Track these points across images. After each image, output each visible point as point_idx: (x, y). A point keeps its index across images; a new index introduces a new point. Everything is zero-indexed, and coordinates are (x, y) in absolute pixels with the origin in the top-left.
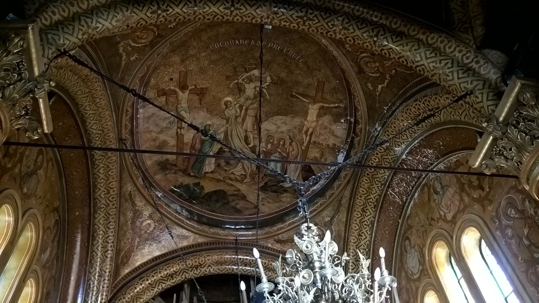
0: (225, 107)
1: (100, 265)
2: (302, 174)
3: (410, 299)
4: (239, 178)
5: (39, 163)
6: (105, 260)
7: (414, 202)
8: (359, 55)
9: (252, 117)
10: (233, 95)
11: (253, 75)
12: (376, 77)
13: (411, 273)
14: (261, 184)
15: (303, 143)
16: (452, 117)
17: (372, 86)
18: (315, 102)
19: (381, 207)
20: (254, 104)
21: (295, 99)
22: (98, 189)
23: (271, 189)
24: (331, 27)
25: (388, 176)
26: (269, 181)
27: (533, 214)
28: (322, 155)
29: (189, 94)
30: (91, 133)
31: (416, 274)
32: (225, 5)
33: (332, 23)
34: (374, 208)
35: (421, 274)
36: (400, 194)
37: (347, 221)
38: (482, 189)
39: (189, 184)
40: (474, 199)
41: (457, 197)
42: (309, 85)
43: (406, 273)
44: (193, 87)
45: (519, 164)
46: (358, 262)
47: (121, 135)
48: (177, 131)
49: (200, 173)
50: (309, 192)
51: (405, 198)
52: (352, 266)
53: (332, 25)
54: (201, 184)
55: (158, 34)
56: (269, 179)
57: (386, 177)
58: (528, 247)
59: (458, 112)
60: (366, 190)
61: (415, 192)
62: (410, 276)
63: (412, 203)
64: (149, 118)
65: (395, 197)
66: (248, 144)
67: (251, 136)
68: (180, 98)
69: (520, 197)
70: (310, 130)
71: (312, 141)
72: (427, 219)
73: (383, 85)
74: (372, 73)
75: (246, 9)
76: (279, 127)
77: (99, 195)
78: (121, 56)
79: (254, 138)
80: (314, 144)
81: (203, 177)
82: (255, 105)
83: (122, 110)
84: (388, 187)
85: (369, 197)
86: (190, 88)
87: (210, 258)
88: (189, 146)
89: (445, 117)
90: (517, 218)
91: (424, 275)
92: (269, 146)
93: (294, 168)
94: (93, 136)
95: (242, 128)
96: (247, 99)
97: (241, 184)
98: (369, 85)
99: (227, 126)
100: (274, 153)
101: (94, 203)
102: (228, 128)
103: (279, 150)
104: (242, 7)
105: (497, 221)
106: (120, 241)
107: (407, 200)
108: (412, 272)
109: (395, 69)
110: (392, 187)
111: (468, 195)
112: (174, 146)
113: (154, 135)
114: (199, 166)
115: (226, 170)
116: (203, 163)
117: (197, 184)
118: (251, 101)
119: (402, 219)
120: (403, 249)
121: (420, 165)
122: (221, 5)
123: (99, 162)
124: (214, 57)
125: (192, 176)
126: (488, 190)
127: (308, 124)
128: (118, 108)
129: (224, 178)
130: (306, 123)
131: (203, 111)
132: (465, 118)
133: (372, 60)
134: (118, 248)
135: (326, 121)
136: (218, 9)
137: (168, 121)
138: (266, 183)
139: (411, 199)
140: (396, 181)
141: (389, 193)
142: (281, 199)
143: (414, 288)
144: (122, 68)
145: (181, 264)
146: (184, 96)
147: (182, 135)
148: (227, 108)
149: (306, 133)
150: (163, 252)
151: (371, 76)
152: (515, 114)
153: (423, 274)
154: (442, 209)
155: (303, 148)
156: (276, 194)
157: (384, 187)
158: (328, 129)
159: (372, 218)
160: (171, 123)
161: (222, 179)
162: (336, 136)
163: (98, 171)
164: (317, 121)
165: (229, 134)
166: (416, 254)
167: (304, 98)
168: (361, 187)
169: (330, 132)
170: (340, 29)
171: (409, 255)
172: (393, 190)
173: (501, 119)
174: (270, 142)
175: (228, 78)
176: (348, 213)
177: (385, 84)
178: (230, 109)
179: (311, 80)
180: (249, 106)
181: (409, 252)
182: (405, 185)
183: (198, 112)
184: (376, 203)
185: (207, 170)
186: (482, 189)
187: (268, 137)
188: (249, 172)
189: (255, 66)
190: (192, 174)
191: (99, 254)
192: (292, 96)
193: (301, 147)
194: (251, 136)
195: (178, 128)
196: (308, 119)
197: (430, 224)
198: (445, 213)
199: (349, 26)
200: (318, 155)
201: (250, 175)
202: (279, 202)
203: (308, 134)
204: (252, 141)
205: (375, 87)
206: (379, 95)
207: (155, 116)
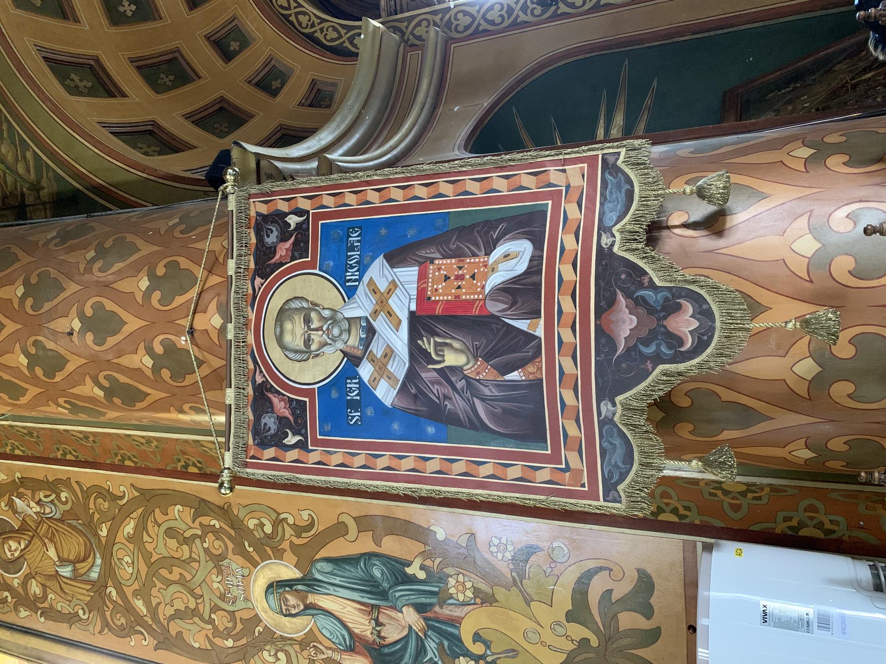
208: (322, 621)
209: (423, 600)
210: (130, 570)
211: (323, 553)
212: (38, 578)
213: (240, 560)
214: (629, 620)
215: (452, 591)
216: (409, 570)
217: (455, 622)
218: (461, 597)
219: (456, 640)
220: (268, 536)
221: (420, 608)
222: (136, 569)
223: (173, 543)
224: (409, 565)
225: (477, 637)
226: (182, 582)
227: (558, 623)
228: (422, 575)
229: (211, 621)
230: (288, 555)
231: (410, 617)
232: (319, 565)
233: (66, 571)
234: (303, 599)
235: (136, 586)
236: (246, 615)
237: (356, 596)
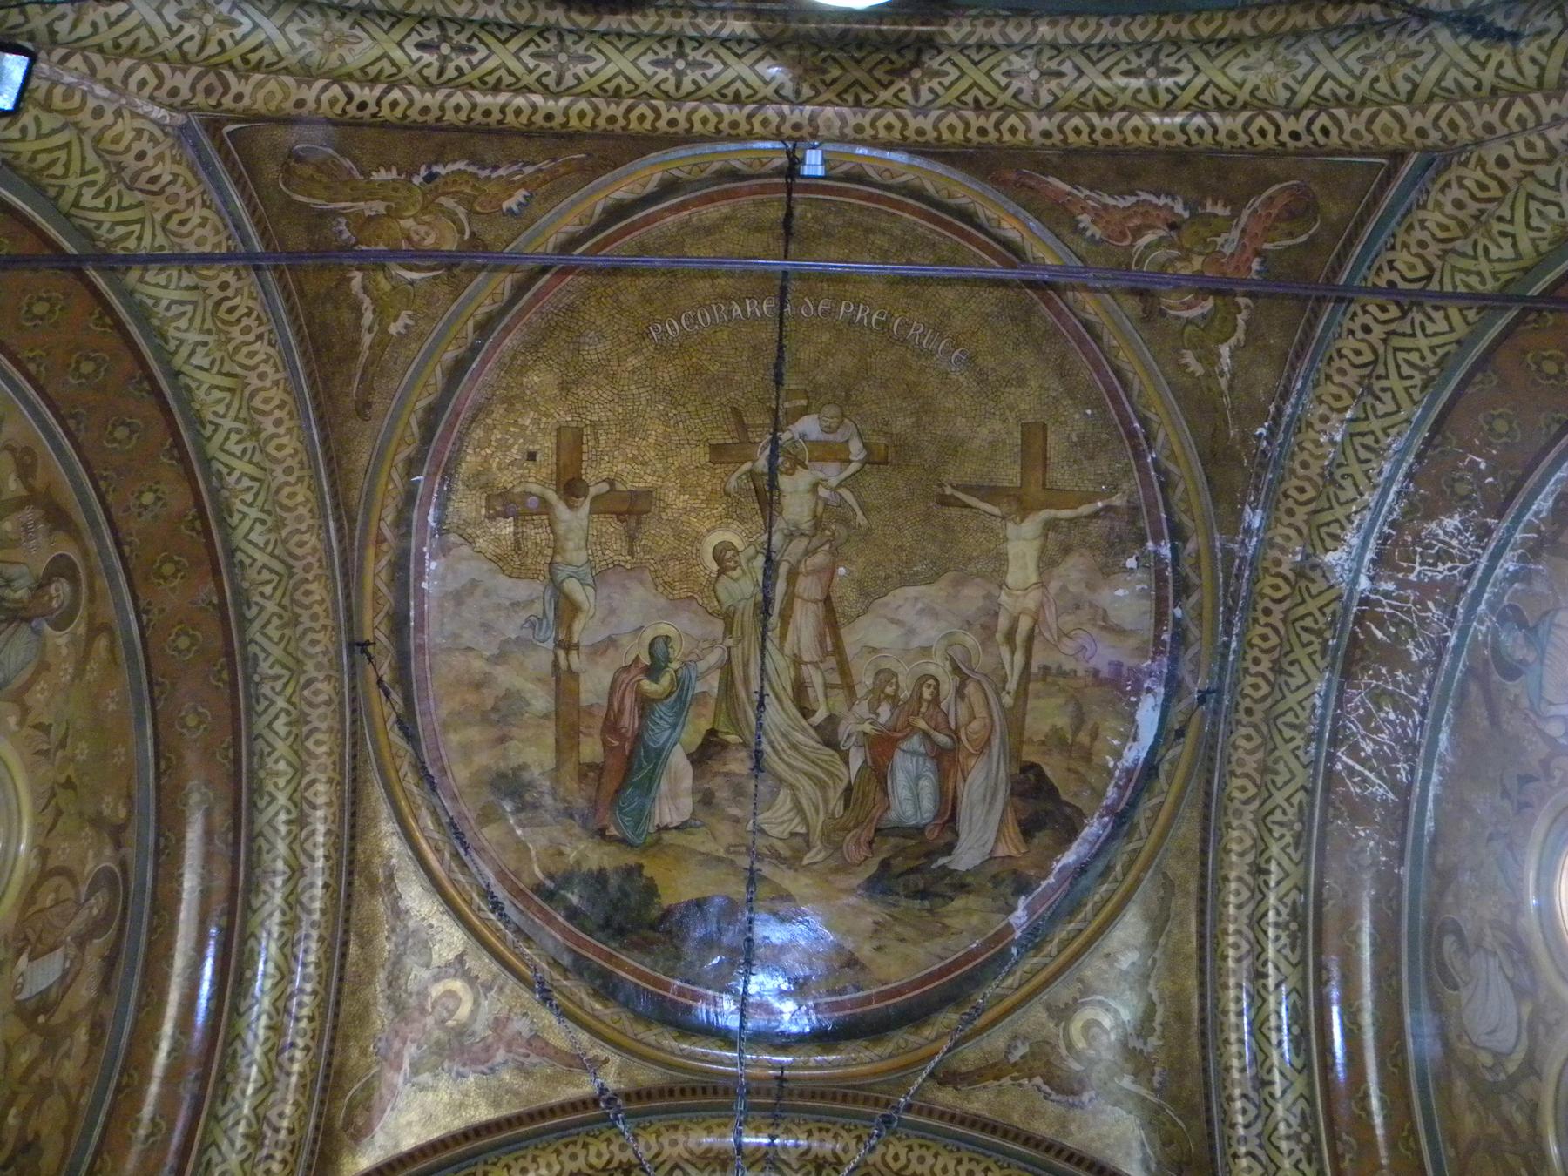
0: (715, 567)
1: (257, 1091)
2: (1016, 811)
4: (785, 852)
5: (55, 604)
6: (275, 1080)
7: (1441, 773)
8: (1132, 245)
9: (812, 607)
10: (742, 520)
11: (803, 436)
12: (1204, 316)
14: (873, 867)
15: (1004, 680)
17: (1199, 360)
18: (1024, 509)
20: (815, 552)
21: (954, 512)
22: (267, 798)
23: (906, 886)
24: (1003, 81)
25: (1326, 698)
26: (899, 851)
28: (1079, 719)
29: (591, 512)
30: (248, 561)
32: (656, 53)
33: (1004, 66)
34: (1296, 848)
36: (1384, 761)
37: (1201, 947)
39: (602, 871)
42: (993, 445)
44: (605, 487)
46: (1268, 1089)
47: (361, 630)
48: (556, 656)
49: (639, 830)
50: (1051, 880)
51: (1403, 776)
52: (1244, 1112)
53: (1007, 74)
54: (647, 872)
55: (473, 234)
56: (896, 846)
57: (1318, 702)
60: (1254, 783)
61: (1436, 729)
63: (1435, 778)
64: (459, 597)
65: (1365, 780)
66: (806, 713)
67: (817, 680)
68: (561, 529)
70: (1024, 624)
71: (1034, 669)
73: (1232, 341)
74: (1190, 307)
75: (724, 63)
76: (911, 632)
77: (270, 823)
78: (357, 309)
79: (827, 686)
80: (1044, 680)
81: (652, 846)
82: (820, 559)
83: (366, 524)
84: (1335, 742)
85: (1269, 806)
86: (593, 491)
87: (680, 1136)
88: (598, 723)
92: (885, 712)
93: (981, 790)
94: (252, 573)
95: (781, 650)
96: (790, 536)
97: (791, 873)
98: (1189, 357)
99: (730, 642)
100: (905, 738)
101: (250, 851)
102: (734, 651)
103: (922, 724)
104: (711, 59)
106: (346, 1038)
107: (1412, 771)
109: (1258, 253)
110: (1346, 738)
112: (546, 716)
113: (478, 665)
114: (637, 801)
115: (736, 820)
116: (650, 789)
117: (632, 872)
118: (805, 541)
119: (1408, 862)
120: (1434, 971)
121: (1430, 604)
122: (645, 53)
123: (273, 689)
124: (668, 373)
125: (612, 840)
127: (1010, 601)
128: (352, 520)
129: (727, 851)
130: (1004, 598)
131: (642, 582)
133: (1176, 253)
134: (336, 1061)
135: (1074, 575)
136: (634, 62)
137: (524, 615)
138: (885, 865)
139: (1428, 764)
140: (1356, 708)
141: (1339, 767)
142: (947, 921)
144: (362, 360)
145: (566, 1153)
146: (574, 520)
147: (573, 675)
148: (722, 571)
149: (1010, 636)
150: (504, 1112)
151: (1189, 321)
155: (1008, 700)
156: (927, 904)
157: (1318, 748)
158: (1086, 606)
159: (1294, 894)
160: (533, 626)
161: (721, 853)
162: (1118, 631)
163: (269, 725)
164: (1042, 584)
165: (738, 672)
167: (982, 499)
168: (1233, 773)
169: (1093, 620)
170: (1034, 82)
172: (1354, 751)
174: (888, 696)
175: (719, 453)
176: (1201, 913)
177: (1240, 334)
178: (735, 574)
179: (998, 426)
180: (799, 562)
182: (1392, 716)
183: (624, 586)
184: (1297, 826)
185: (667, 820)
187: (877, 674)
188: (818, 821)
189: (804, 402)
190: (613, 831)
191: (258, 1053)
192: (945, 501)
193: (999, 699)
194: (817, 680)
195: (559, 644)
196: (1010, 580)
199: (1060, 64)
200: (1063, 721)
201: (826, 837)
202: (940, 935)
203: (1020, 638)
204: (821, 698)
205: (1210, 358)
206: (1231, 388)
207: (479, 592)
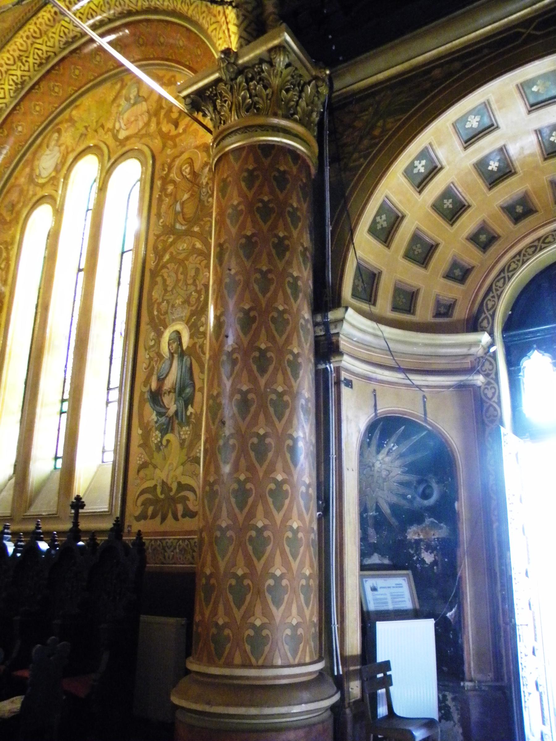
3: (18, 202)
13: (37, 174)
16: (201, 18)
19: (48, 72)
27: (204, 184)
31: (42, 178)
35: (48, 182)
38: (176, 125)
40: (160, 132)
41: (145, 118)
43: (32, 170)
45: (222, 122)
58: (176, 213)
59: (211, 19)
62: (34, 176)
69: (206, 159)
72: (97, 122)
89: (194, 12)
90: (187, 178)
91: (53, 184)
105: (166, 169)
108: (40, 174)
111: (158, 123)
126: (181, 131)
132: (212, 31)
143: (31, 193)
152: (257, 66)
153: (52, 182)
154: (121, 121)
166: (58, 155)
171: (48, 152)
173: (240, 62)
181: (51, 147)
186: (176, 125)
197: (96, 131)
198: (120, 128)
208: (168, 363)
209: (179, 414)
210: (181, 248)
211: (194, 361)
212: (174, 190)
213: (188, 314)
214: (180, 507)
215: (184, 429)
216: (190, 407)
217: (172, 430)
218: (182, 433)
219: (166, 433)
220: (198, 329)
221: (176, 413)
222: (181, 252)
223: (192, 273)
224: (192, 407)
225: (168, 441)
226: (178, 281)
227: (176, 478)
228: (188, 414)
229: (163, 302)
230: (192, 342)
231: (173, 408)
232: (189, 359)
233: (178, 208)
234: (176, 352)
235: (175, 253)
236: (167, 320)
237: (178, 380)
